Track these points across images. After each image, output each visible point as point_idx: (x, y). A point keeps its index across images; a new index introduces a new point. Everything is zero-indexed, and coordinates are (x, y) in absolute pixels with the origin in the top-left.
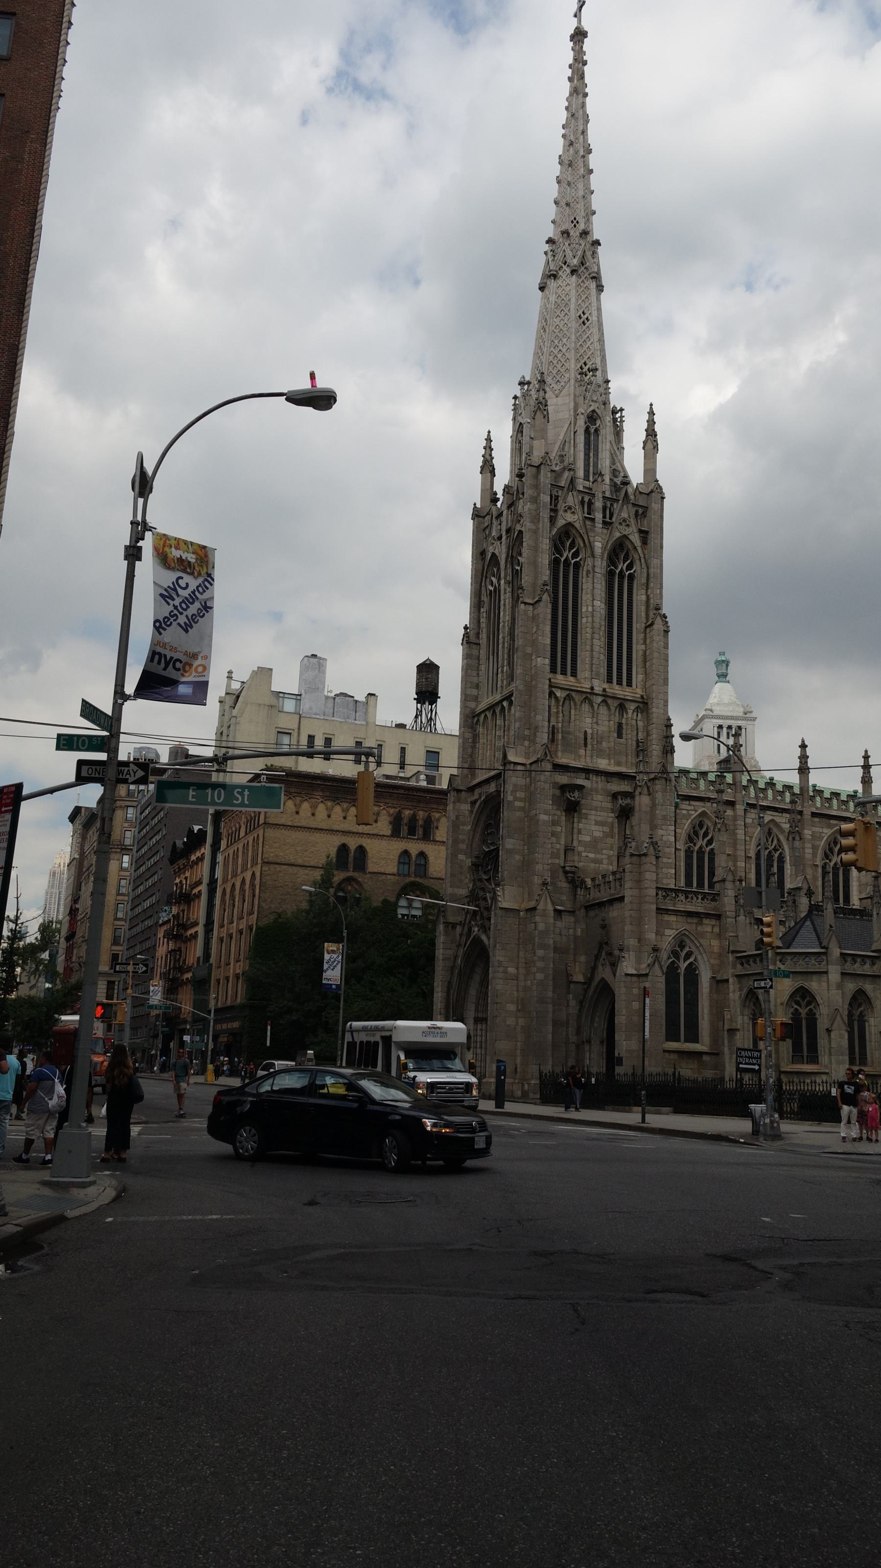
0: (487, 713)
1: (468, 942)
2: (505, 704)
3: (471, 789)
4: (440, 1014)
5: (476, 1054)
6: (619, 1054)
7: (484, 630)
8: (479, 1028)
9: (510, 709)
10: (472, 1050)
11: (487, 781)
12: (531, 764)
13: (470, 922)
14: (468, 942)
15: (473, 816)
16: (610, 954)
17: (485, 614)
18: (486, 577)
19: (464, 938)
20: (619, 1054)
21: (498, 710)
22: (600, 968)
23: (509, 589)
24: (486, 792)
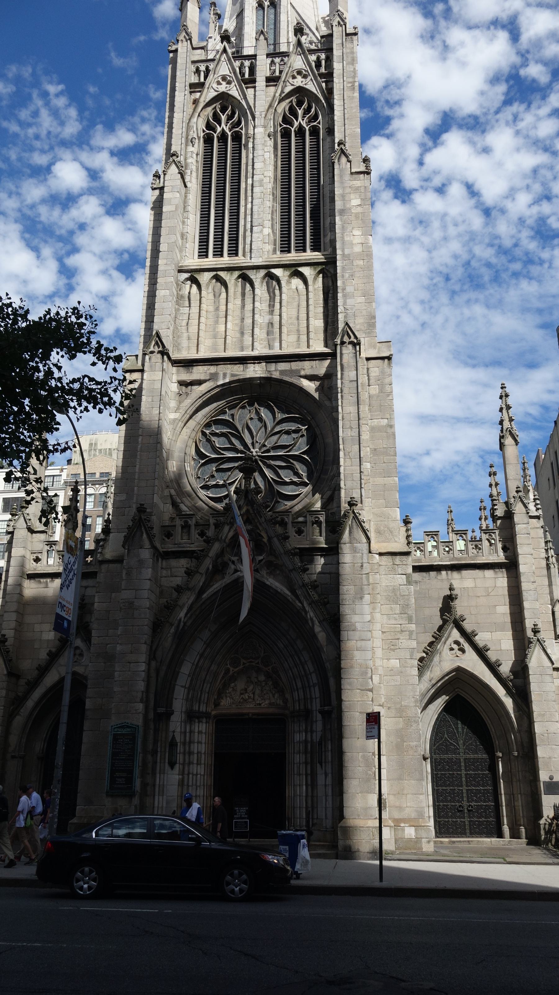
0: (222, 274)
1: (217, 586)
2: (278, 272)
3: (188, 364)
4: (141, 701)
5: (193, 775)
6: (551, 778)
7: (194, 174)
8: (196, 730)
9: (289, 282)
10: (177, 766)
11: (243, 361)
12: (368, 359)
13: (221, 554)
14: (217, 586)
15: (188, 402)
16: (469, 637)
17: (195, 156)
18: (199, 115)
19: (199, 580)
20: (551, 778)
21: (257, 277)
22: (446, 652)
23: (271, 143)
24: (233, 375)
